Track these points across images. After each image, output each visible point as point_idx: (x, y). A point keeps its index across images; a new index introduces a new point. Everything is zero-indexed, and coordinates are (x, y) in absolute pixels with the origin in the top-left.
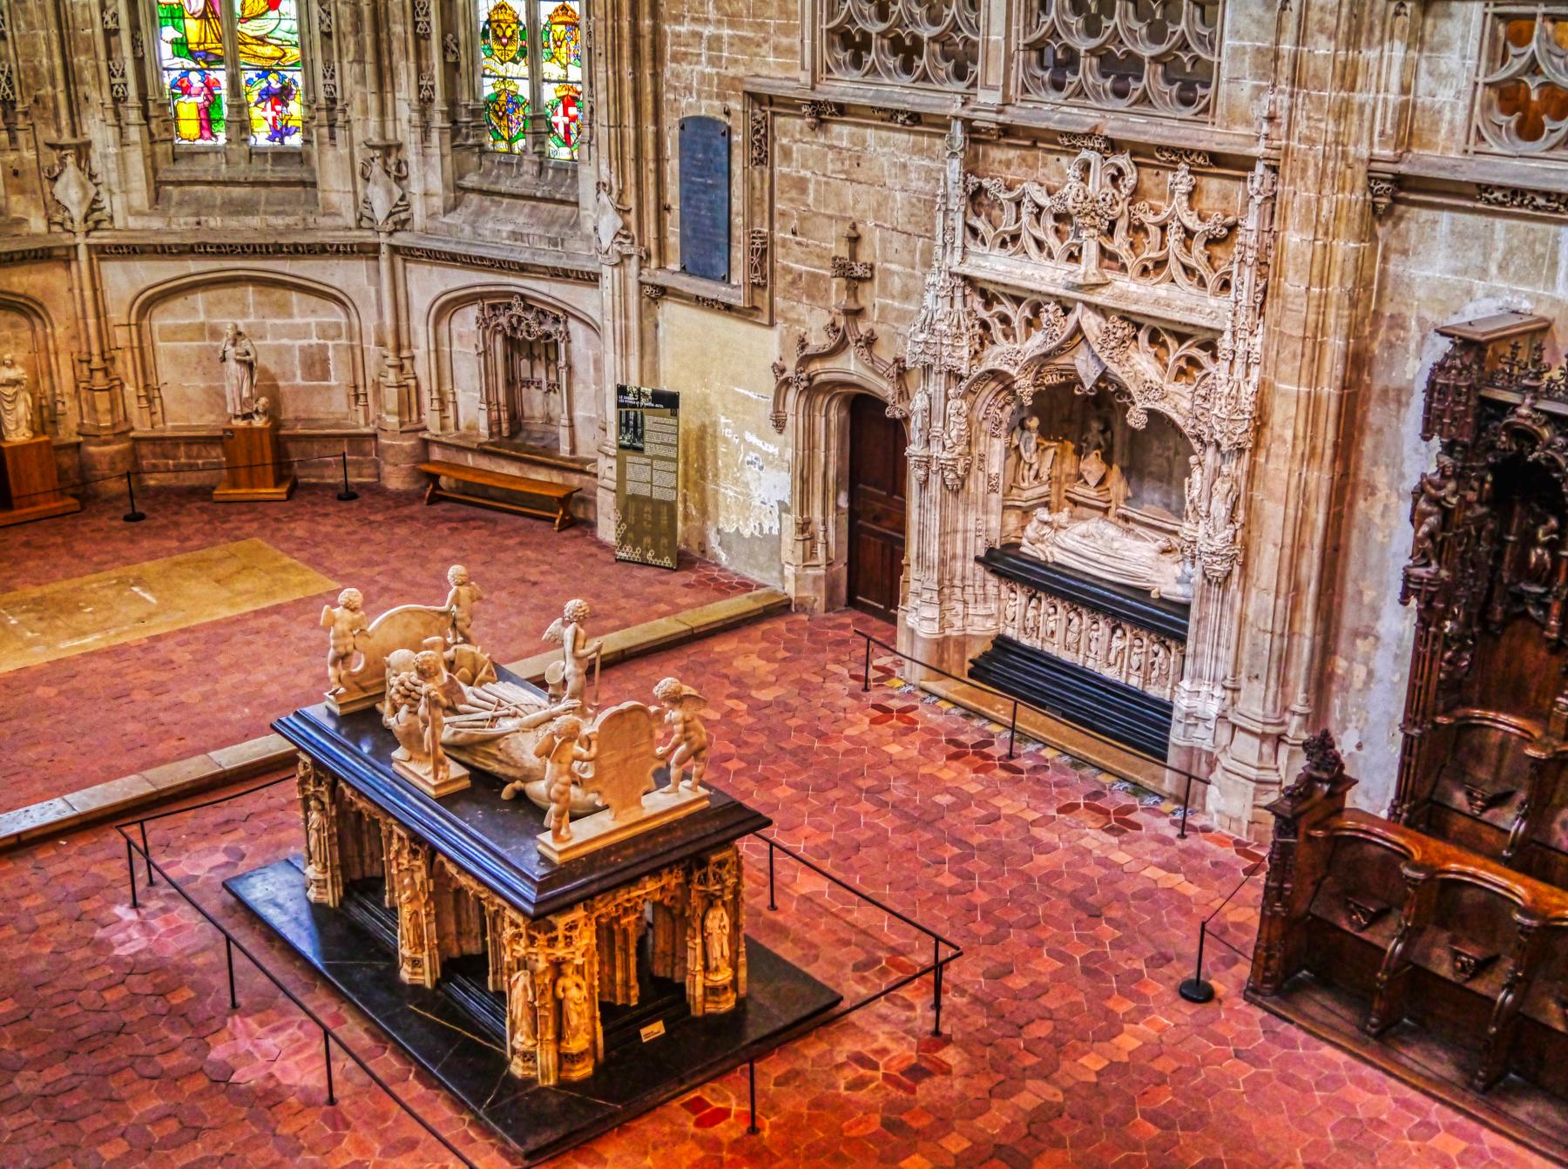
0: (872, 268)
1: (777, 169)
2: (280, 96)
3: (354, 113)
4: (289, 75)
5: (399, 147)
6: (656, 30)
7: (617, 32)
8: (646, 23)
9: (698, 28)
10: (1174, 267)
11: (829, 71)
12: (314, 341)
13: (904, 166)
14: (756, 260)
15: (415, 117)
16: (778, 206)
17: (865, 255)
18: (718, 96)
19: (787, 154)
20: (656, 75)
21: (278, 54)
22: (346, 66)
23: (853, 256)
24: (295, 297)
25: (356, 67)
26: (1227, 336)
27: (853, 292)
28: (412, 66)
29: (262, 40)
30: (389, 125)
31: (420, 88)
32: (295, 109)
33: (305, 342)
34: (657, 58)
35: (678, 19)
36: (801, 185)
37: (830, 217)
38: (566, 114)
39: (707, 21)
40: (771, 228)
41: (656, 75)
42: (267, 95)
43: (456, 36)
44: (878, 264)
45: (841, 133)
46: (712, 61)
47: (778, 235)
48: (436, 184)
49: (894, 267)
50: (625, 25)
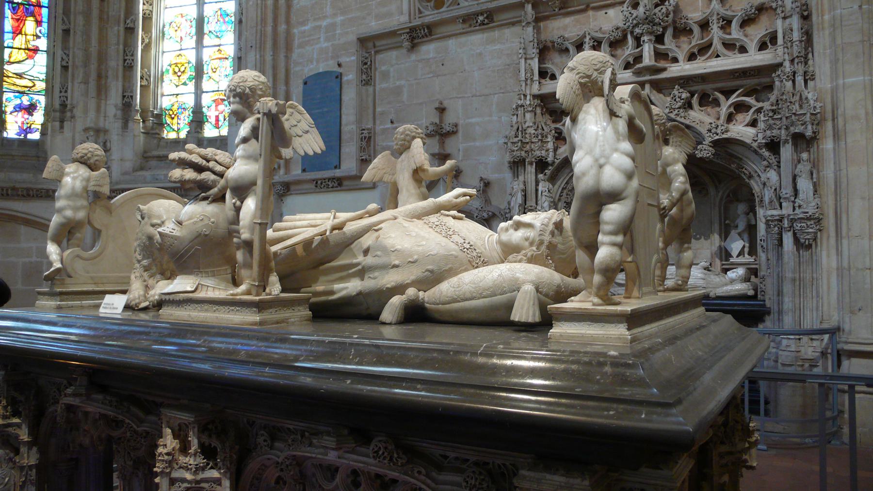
0: (456, 125)
1: (378, 87)
2: (30, 109)
3: (78, 112)
4: (36, 97)
5: (106, 131)
6: (288, 32)
7: (263, 34)
8: (282, 28)
9: (318, 23)
10: (717, 45)
11: (420, 12)
12: (34, 259)
13: (480, 54)
14: (364, 143)
15: (119, 113)
16: (378, 109)
17: (450, 118)
18: (332, 58)
19: (386, 76)
20: (287, 58)
21: (30, 84)
22: (76, 85)
23: (441, 121)
24: (23, 229)
25: (83, 86)
26: (787, 64)
27: (442, 143)
28: (120, 84)
29: (20, 76)
30: (102, 119)
31: (124, 97)
32: (38, 118)
33: (27, 260)
34: (289, 48)
35: (303, 23)
36: (398, 91)
37: (421, 104)
38: (217, 110)
39: (325, 17)
40: (374, 123)
41: (287, 58)
42: (19, 108)
43: (149, 71)
44: (461, 122)
45: (429, 50)
46: (327, 39)
47: (379, 128)
48: (129, 154)
49: (473, 120)
50: (269, 29)
